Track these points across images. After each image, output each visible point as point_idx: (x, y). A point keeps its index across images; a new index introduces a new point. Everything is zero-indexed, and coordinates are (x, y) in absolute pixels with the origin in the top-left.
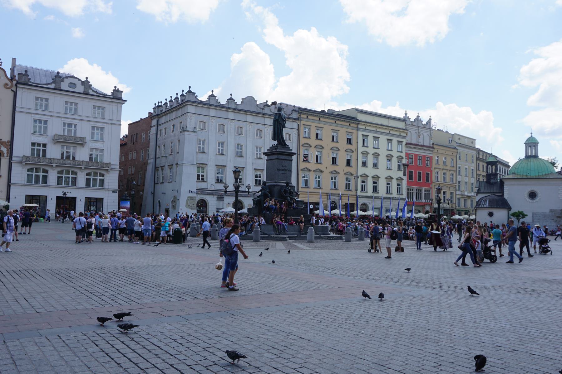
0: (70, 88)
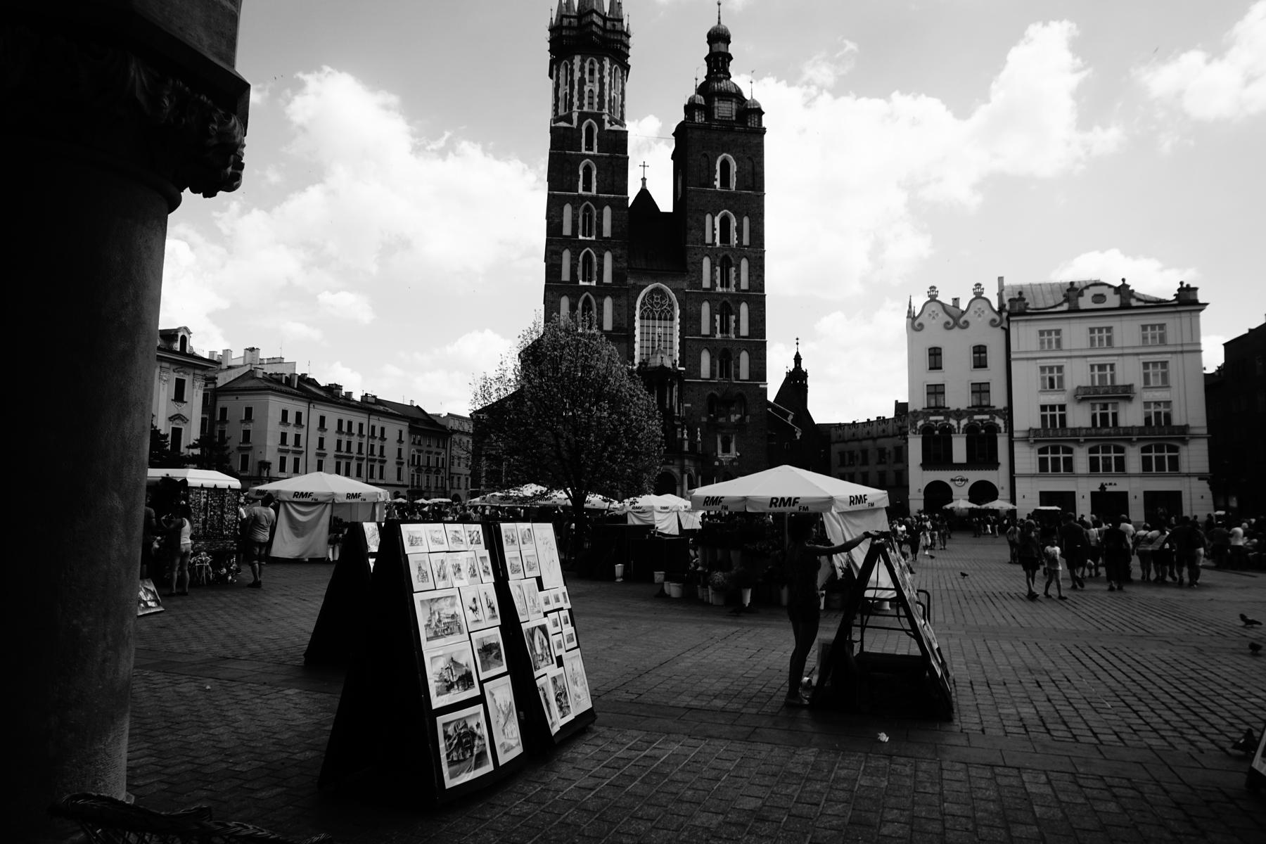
0: (1096, 302)
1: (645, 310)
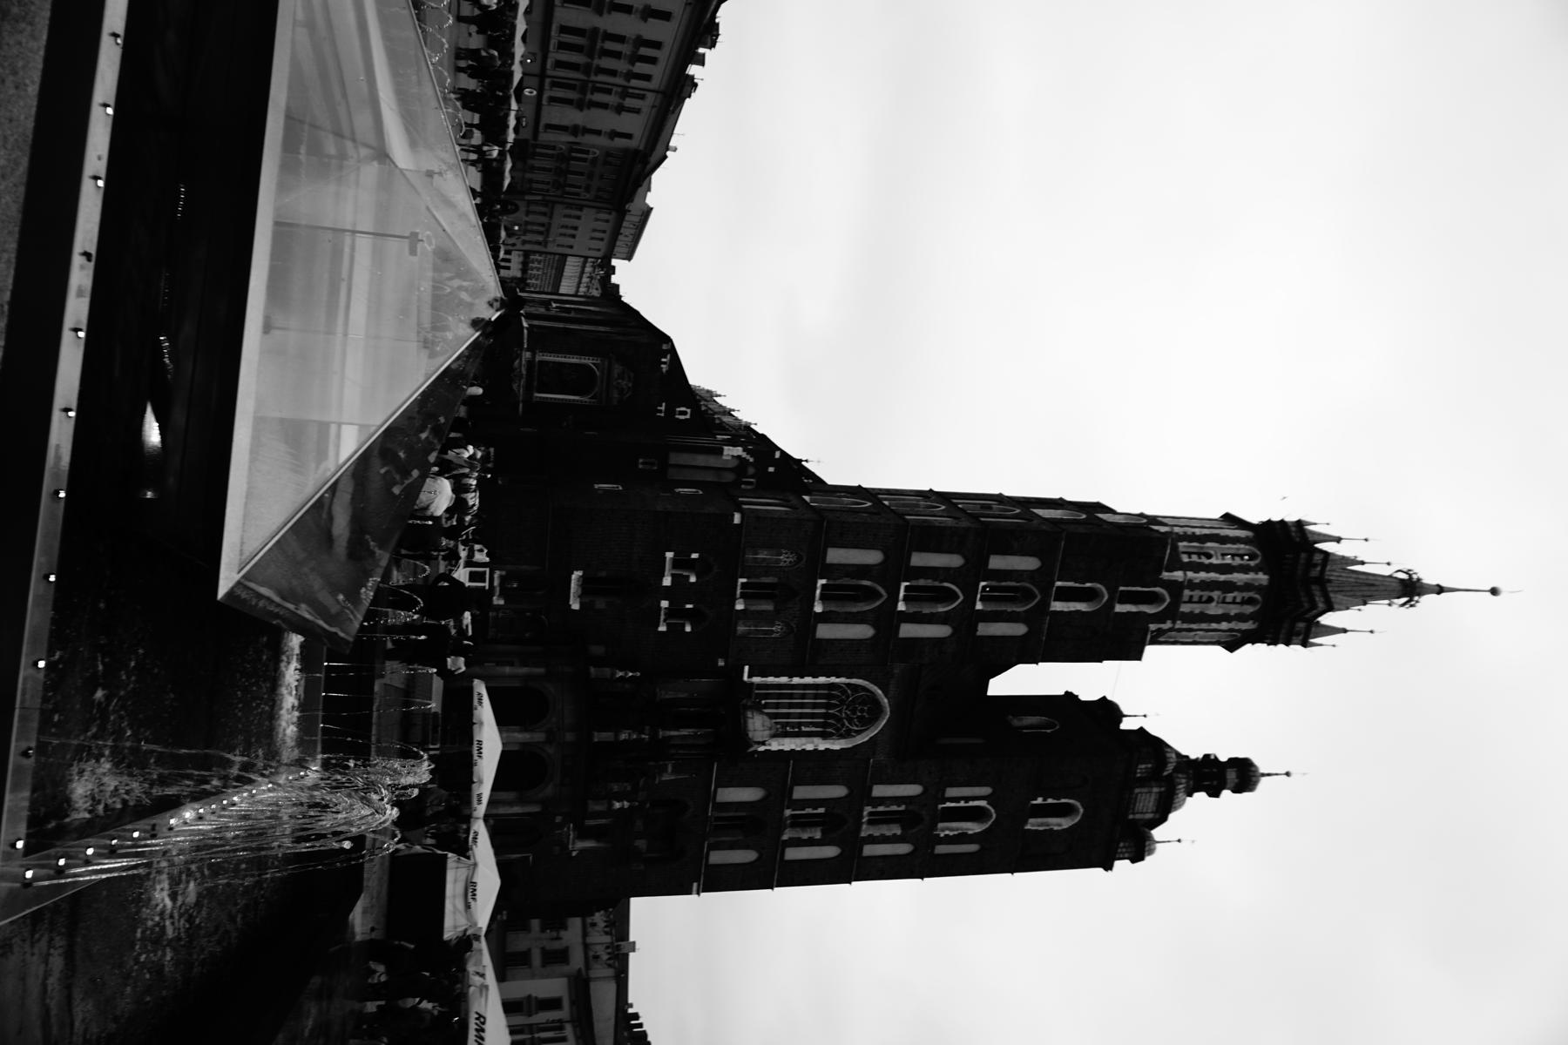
1: (844, 692)
